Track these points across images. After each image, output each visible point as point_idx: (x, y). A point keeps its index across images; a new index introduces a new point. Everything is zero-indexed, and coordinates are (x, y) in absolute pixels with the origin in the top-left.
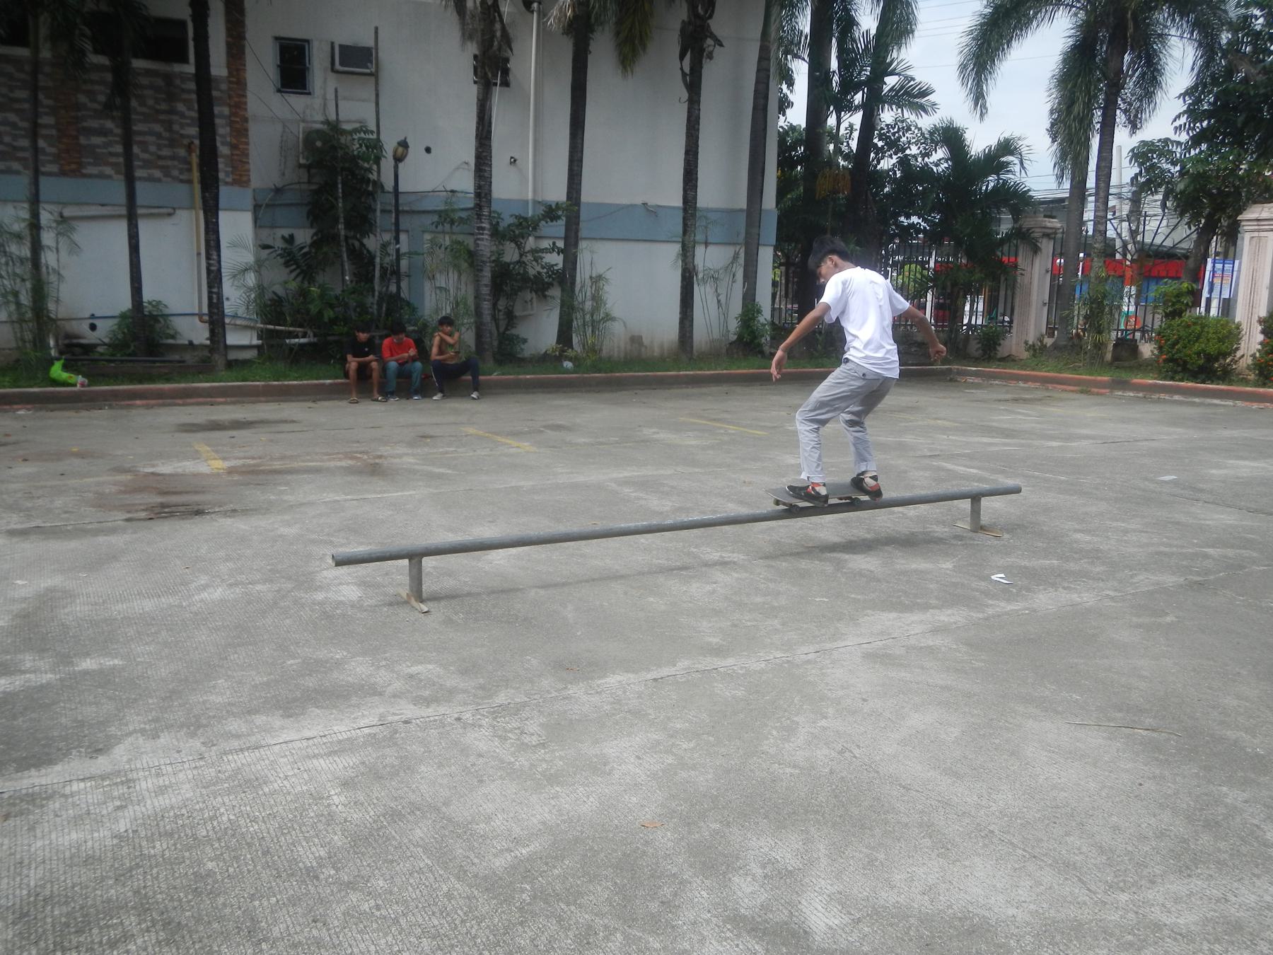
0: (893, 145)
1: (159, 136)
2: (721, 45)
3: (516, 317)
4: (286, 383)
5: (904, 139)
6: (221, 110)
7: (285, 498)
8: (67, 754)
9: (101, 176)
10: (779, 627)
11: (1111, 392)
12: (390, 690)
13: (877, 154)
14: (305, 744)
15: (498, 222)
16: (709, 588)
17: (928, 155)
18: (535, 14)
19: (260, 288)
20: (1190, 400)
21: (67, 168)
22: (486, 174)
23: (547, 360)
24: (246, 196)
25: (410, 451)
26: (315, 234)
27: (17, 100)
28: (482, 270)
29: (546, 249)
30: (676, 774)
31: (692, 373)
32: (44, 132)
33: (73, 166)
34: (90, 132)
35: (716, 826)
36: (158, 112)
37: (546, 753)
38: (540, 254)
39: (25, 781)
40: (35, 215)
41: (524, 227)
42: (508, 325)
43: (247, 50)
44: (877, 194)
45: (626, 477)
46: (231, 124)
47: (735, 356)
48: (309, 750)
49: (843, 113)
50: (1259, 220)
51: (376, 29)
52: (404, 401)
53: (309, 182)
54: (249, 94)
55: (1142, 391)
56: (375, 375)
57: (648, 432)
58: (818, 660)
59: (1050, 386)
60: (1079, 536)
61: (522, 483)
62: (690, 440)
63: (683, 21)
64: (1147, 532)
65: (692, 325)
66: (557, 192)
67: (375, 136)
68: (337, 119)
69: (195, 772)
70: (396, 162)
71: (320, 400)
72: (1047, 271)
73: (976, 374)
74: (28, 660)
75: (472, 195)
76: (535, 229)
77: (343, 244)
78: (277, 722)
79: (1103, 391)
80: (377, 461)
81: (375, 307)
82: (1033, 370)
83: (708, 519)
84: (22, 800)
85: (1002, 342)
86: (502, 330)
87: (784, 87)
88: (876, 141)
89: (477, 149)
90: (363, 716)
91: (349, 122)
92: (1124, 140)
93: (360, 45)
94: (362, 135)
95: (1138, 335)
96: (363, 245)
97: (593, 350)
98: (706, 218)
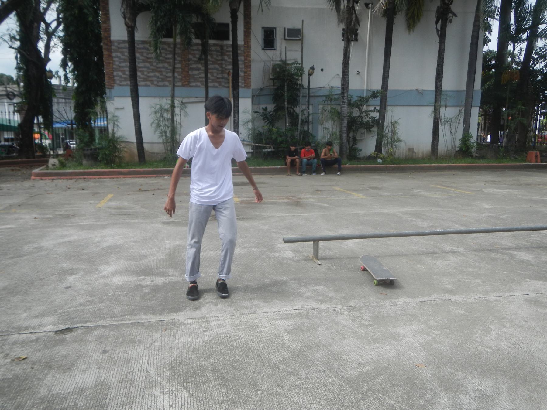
1: (218, 69)
2: (456, 16)
3: (357, 140)
4: (262, 167)
6: (241, 58)
7: (262, 214)
8: (186, 308)
9: (197, 86)
10: (481, 283)
12: (306, 295)
13: (534, 62)
14: (273, 314)
15: (351, 100)
16: (446, 263)
18: (370, 9)
19: (254, 129)
21: (184, 83)
22: (346, 79)
23: (370, 159)
24: (249, 92)
26: (275, 107)
27: (168, 59)
28: (343, 120)
29: (372, 110)
30: (431, 345)
32: (177, 70)
33: (187, 83)
34: (193, 69)
35: (452, 370)
36: (217, 60)
37: (372, 329)
39: (172, 317)
40: (173, 102)
41: (362, 101)
42: (353, 143)
43: (252, 33)
44: (533, 80)
46: (245, 63)
47: (459, 157)
48: (274, 317)
49: (516, 44)
51: (303, 21)
52: (309, 175)
53: (274, 86)
54: (252, 51)
56: (298, 164)
57: (416, 191)
58: (501, 300)
61: (360, 212)
62: (436, 195)
63: (438, 7)
65: (438, 143)
66: (377, 86)
67: (301, 65)
68: (286, 59)
69: (232, 320)
71: (275, 174)
74: (171, 271)
75: (340, 88)
76: (367, 102)
77: (286, 110)
78: (262, 304)
80: (298, 200)
81: (298, 136)
84: (171, 324)
86: (351, 145)
87: (487, 33)
88: (533, 56)
89: (343, 69)
90: (295, 305)
91: (290, 60)
93: (296, 28)
94: (296, 65)
96: (294, 111)
97: (391, 154)
98: (446, 95)
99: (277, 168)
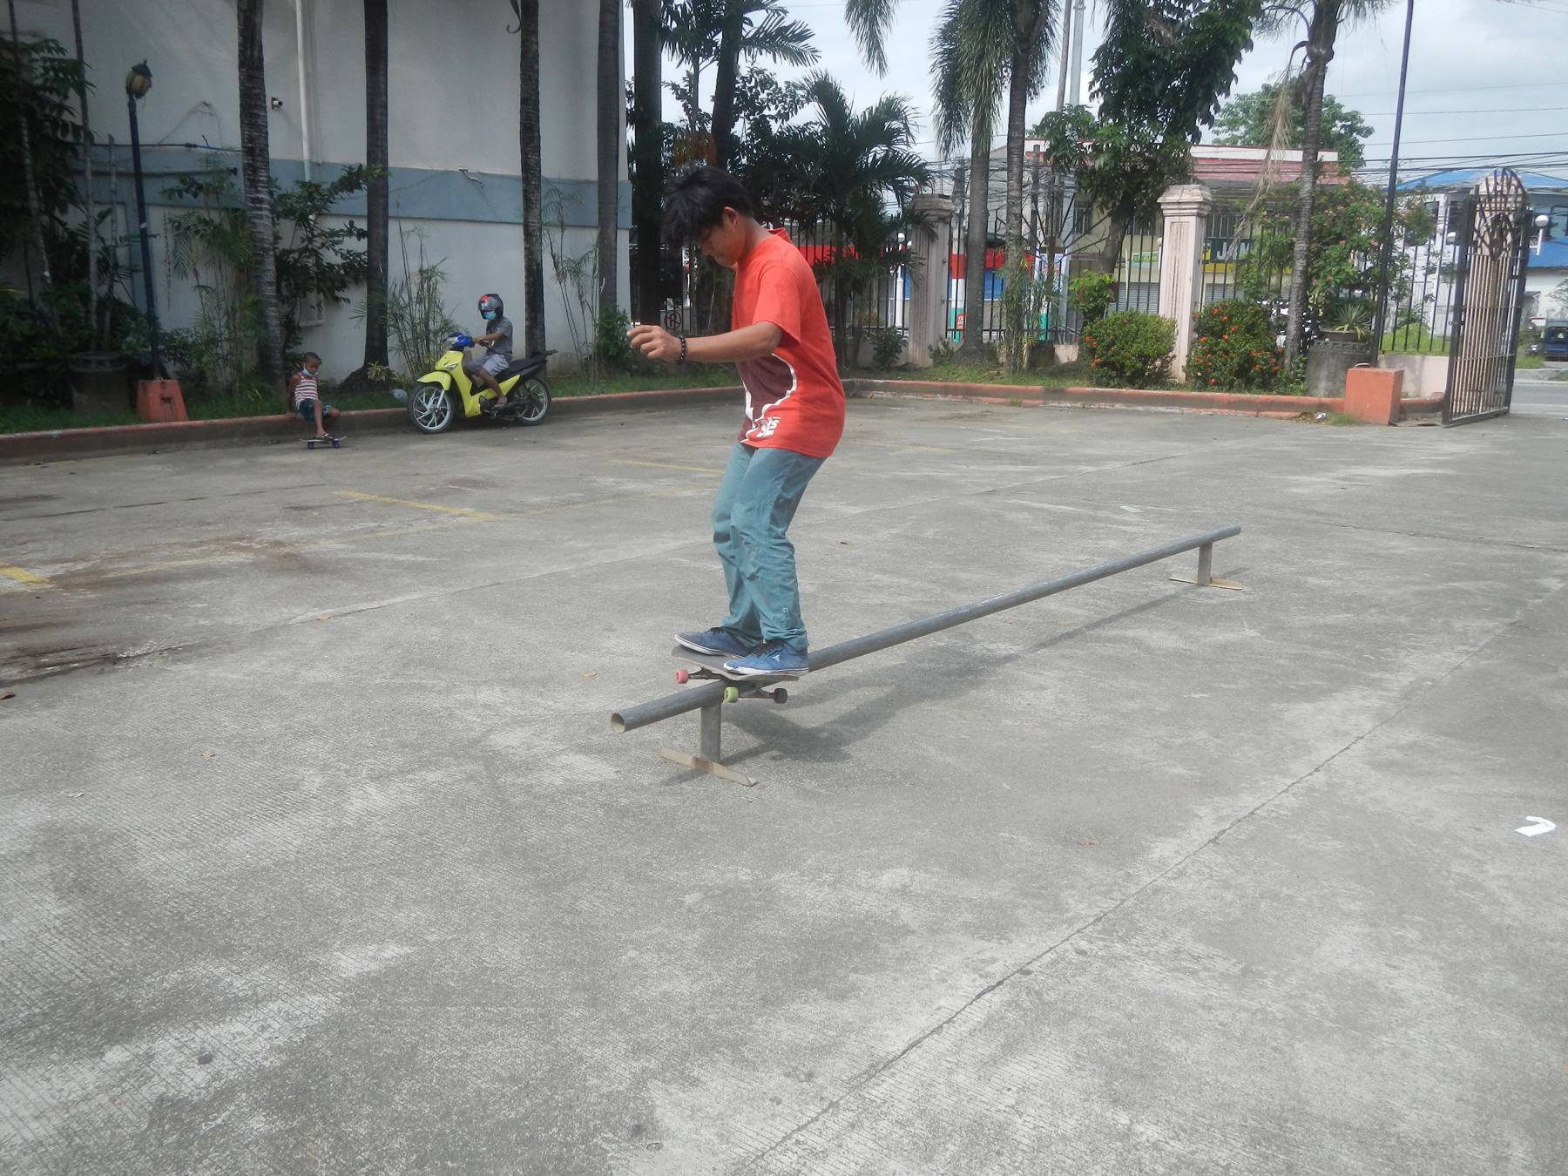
0: (752, 105)
3: (300, 329)
5: (763, 96)
7: (228, 620)
11: (1045, 403)
17: (785, 117)
22: (260, 121)
23: (358, 384)
25: (312, 532)
29: (342, 231)
31: (564, 399)
37: (1277, 980)
38: (336, 239)
50: (1179, 203)
55: (1078, 400)
58: (1335, 780)
60: (1312, 580)
61: (555, 568)
64: (1368, 569)
67: (71, 54)
68: (14, 27)
70: (131, 98)
72: (944, 262)
73: (885, 388)
78: (846, 1012)
79: (1036, 402)
82: (946, 380)
83: (1000, 601)
85: (903, 348)
89: (242, 84)
92: (1038, 109)
94: (46, 54)
99: (50, 437)
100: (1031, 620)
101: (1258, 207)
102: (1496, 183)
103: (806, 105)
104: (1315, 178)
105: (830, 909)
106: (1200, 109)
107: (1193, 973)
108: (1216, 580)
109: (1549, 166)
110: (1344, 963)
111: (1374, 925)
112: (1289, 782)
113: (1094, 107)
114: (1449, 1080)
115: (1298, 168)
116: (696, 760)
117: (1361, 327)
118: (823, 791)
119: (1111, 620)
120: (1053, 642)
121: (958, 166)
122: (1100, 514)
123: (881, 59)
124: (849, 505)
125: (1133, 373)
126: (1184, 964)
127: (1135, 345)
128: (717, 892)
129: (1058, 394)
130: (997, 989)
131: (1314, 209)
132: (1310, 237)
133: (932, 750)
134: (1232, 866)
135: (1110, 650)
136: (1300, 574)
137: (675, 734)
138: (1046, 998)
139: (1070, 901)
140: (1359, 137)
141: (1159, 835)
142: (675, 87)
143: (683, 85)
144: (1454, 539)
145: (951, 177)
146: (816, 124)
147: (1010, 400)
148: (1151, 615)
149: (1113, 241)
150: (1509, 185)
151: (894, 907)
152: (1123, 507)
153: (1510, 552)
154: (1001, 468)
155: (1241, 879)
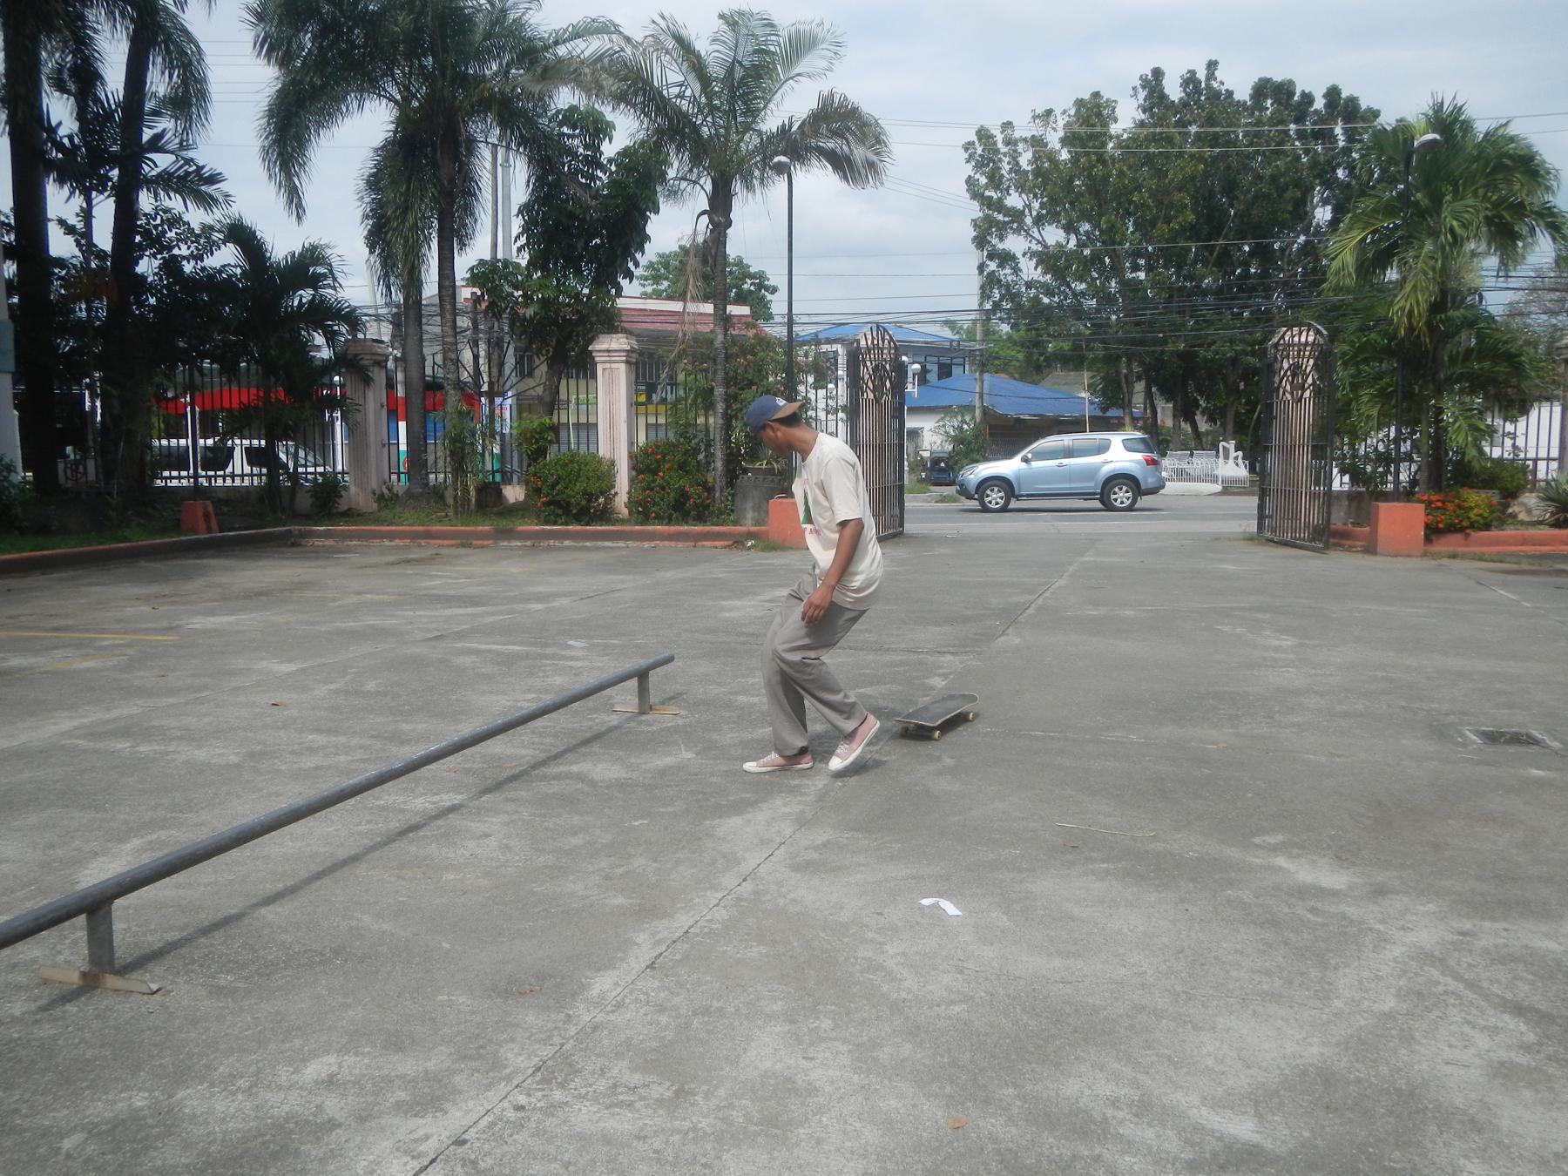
0: (156, 242)
5: (169, 235)
11: (495, 543)
16: (492, 842)
20: (581, 544)
37: (708, 1095)
45: (76, 728)
49: (94, 193)
50: (608, 351)
58: (761, 887)
59: (423, 542)
60: (742, 699)
72: (382, 406)
79: (486, 543)
83: (436, 750)
85: (343, 493)
92: (464, 263)
95: (498, 477)
100: (477, 766)
101: (679, 356)
102: (873, 338)
103: (223, 246)
104: (726, 330)
105: (244, 1119)
106: (620, 267)
107: (629, 1105)
108: (657, 707)
109: (918, 323)
110: (768, 1064)
111: (793, 1022)
112: (719, 895)
113: (523, 260)
114: (855, 1157)
115: (712, 318)
116: (84, 975)
117: (777, 462)
118: (239, 985)
119: (556, 757)
120: (497, 786)
121: (394, 310)
122: (549, 651)
123: (300, 206)
124: (282, 662)
125: (579, 511)
126: (621, 1098)
127: (578, 484)
128: (104, 1127)
129: (509, 534)
130: (430, 1169)
131: (728, 357)
132: (727, 382)
133: (367, 919)
134: (667, 988)
135: (555, 787)
136: (731, 693)
137: (59, 947)
138: (482, 1165)
139: (510, 1055)
140: (766, 294)
141: (599, 970)
142: (62, 222)
143: (73, 220)
144: (861, 649)
145: (388, 321)
146: (235, 266)
147: (459, 541)
148: (596, 747)
149: (550, 385)
150: (883, 342)
151: (318, 1101)
152: (570, 643)
153: (904, 657)
154: (449, 612)
155: (676, 1000)
